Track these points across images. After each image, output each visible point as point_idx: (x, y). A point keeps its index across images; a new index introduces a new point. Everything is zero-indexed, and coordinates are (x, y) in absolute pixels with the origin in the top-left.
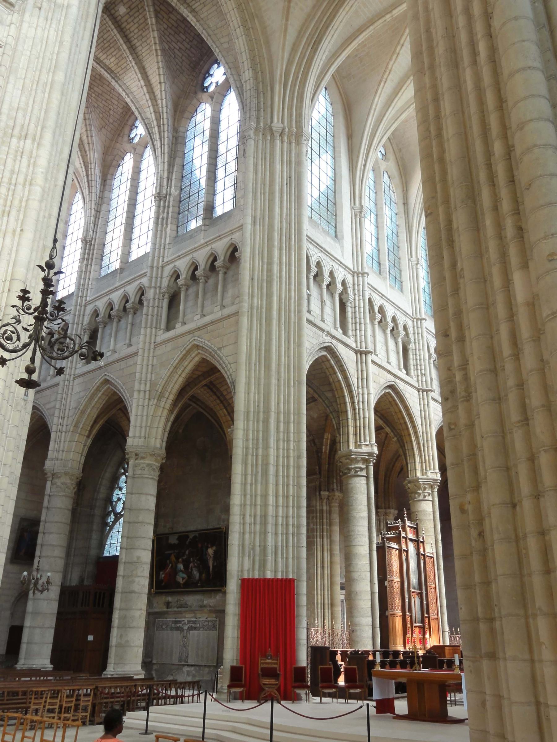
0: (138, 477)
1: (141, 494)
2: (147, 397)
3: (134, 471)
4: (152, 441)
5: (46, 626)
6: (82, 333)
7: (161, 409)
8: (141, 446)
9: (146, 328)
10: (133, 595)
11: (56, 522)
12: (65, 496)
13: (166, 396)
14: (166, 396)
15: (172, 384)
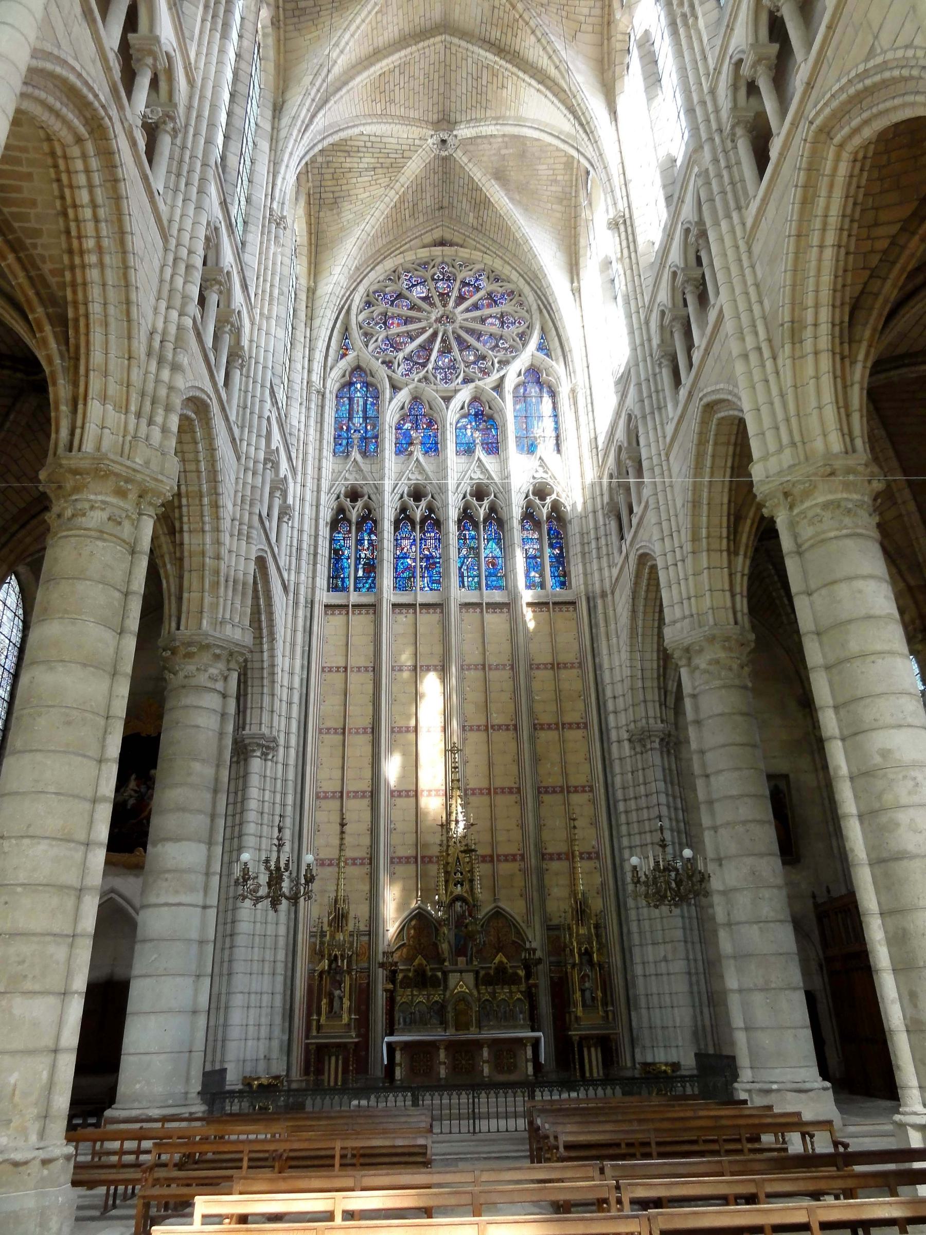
0: (812, 546)
1: (834, 582)
2: (766, 353)
3: (795, 536)
4: (819, 445)
5: (773, 985)
6: (657, 370)
7: (810, 359)
8: (790, 467)
9: (717, 224)
10: (905, 863)
11: (724, 746)
12: (724, 687)
13: (810, 319)
14: (810, 319)
15: (812, 281)
